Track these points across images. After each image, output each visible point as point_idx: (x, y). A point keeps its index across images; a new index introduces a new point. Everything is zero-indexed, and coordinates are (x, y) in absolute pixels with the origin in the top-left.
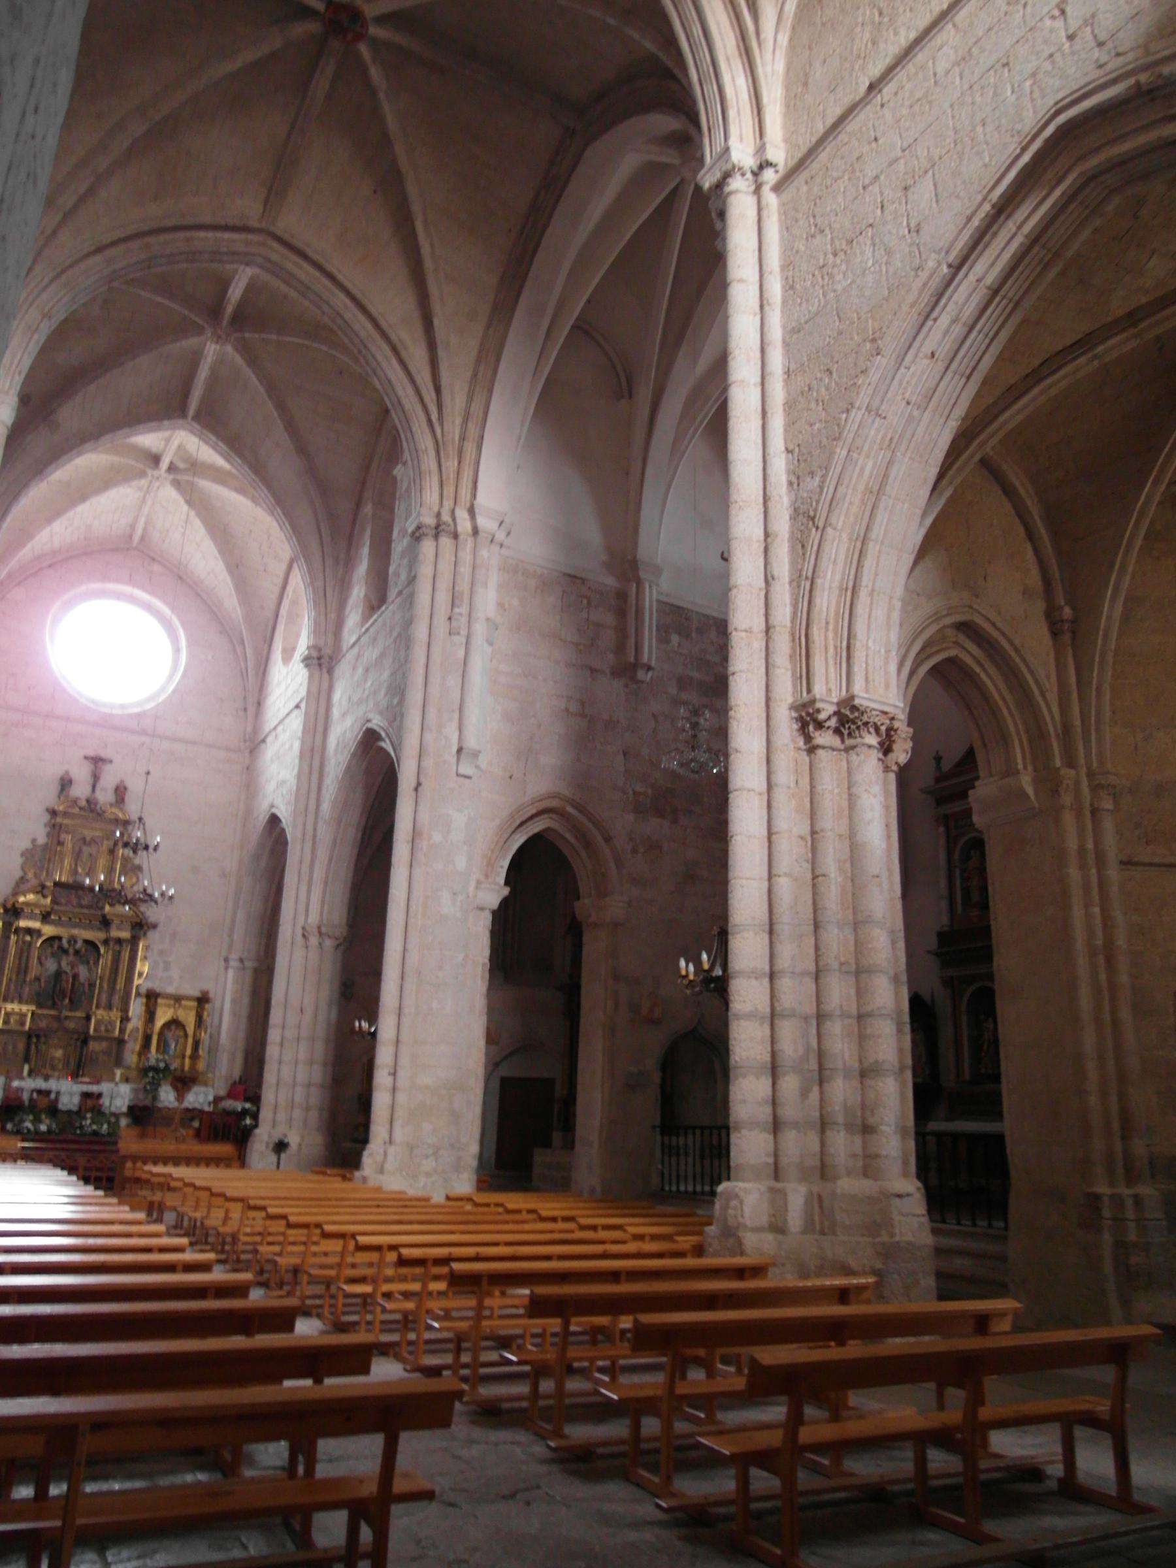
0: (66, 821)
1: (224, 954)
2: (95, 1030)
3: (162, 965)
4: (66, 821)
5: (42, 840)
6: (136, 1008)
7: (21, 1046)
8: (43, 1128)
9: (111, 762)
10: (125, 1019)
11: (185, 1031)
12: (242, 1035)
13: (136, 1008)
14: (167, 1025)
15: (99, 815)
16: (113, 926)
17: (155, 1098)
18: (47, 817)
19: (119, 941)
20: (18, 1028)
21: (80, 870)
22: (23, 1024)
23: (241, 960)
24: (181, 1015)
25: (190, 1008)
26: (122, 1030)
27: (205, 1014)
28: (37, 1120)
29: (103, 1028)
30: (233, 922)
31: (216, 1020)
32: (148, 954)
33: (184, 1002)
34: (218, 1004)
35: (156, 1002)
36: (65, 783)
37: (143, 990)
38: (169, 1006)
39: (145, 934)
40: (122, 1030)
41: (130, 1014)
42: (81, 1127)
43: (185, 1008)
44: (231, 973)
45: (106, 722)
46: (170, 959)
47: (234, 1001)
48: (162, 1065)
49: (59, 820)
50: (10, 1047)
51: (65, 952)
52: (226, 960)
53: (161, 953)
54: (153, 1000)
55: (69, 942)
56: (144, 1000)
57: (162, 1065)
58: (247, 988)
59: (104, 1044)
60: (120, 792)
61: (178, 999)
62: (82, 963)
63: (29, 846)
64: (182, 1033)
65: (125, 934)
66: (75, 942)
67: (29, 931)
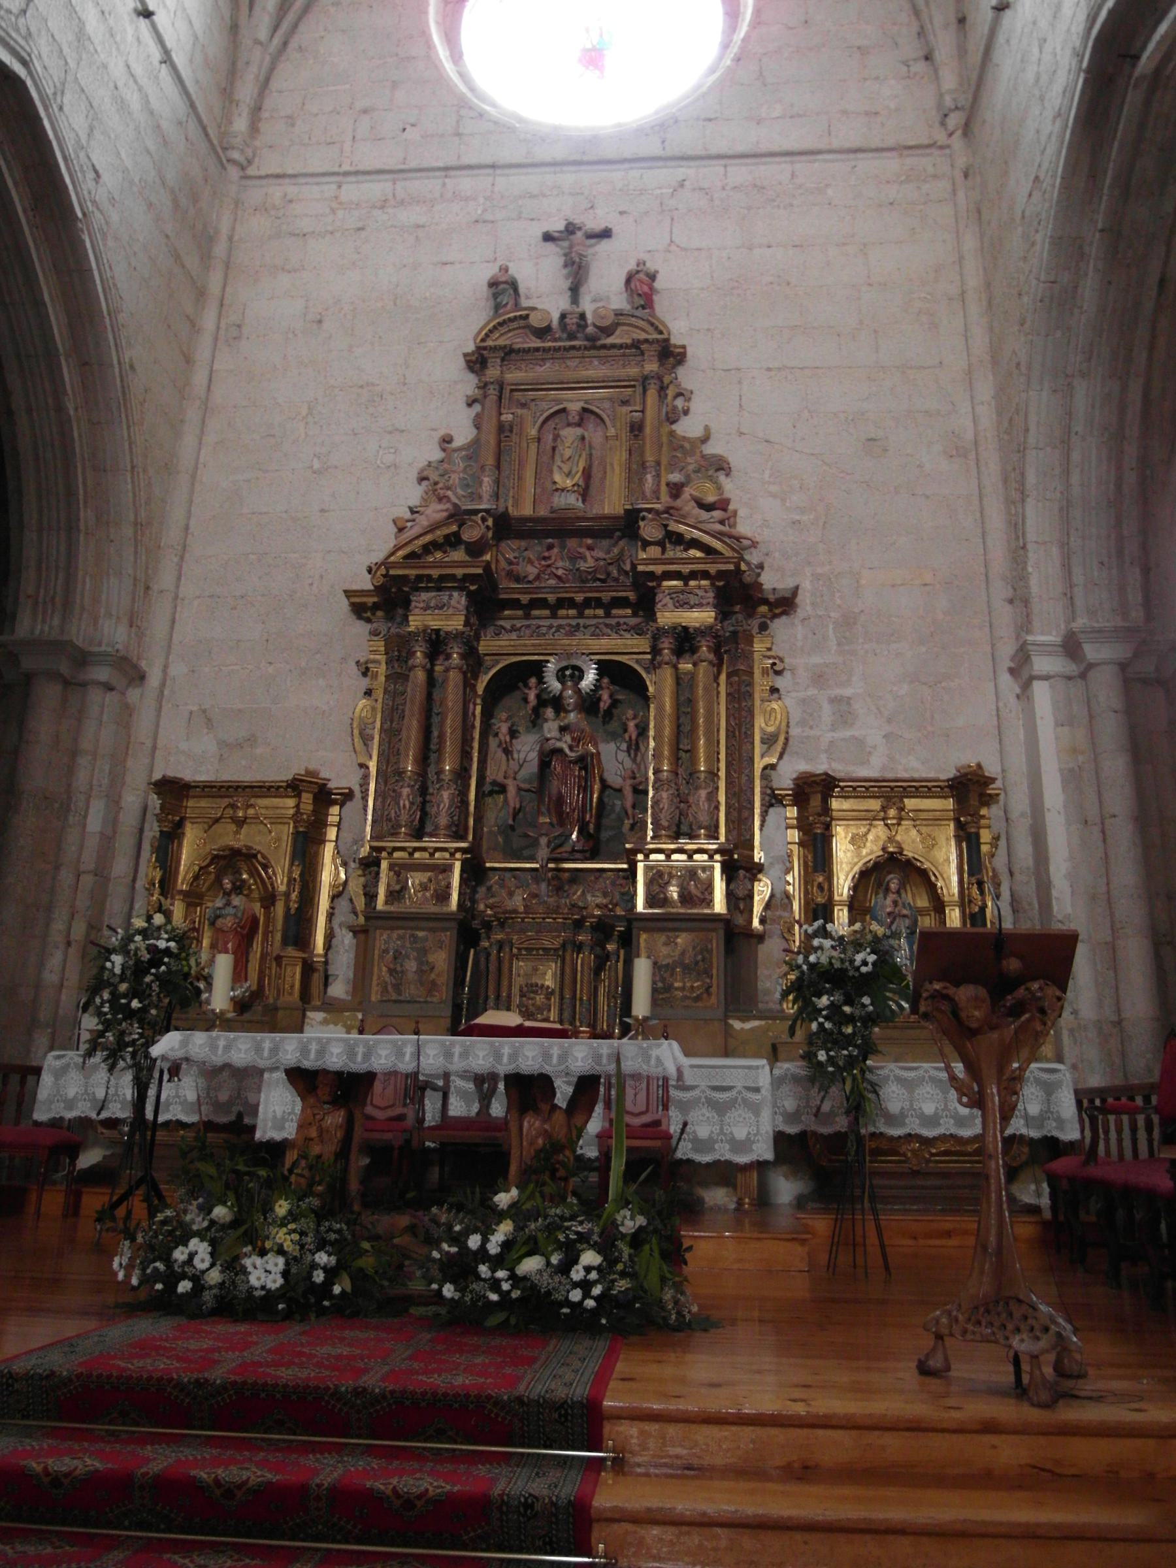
0: (513, 376)
1: (1007, 649)
2: (650, 901)
3: (827, 710)
4: (513, 376)
5: (463, 434)
6: (775, 837)
7: (441, 959)
8: (264, 1273)
9: (606, 234)
10: (741, 869)
11: (932, 888)
12: (1127, 875)
13: (775, 837)
14: (870, 877)
15: (592, 339)
16: (663, 599)
17: (857, 1106)
18: (469, 384)
19: (685, 640)
20: (432, 908)
21: (557, 477)
22: (444, 896)
23: (1071, 647)
24: (910, 841)
25: (936, 820)
26: (739, 900)
27: (985, 836)
28: (246, 1233)
29: (674, 892)
30: (1018, 553)
31: (1024, 850)
32: (780, 682)
33: (910, 803)
34: (1018, 801)
35: (826, 810)
36: (503, 288)
37: (785, 779)
38: (870, 818)
39: (763, 627)
40: (739, 900)
41: (758, 856)
42: (461, 1268)
43: (918, 818)
44: (1041, 691)
45: (587, 156)
46: (848, 692)
47: (1071, 778)
48: (865, 959)
49: (493, 372)
50: (411, 966)
51: (557, 703)
52: (1021, 666)
53: (819, 678)
54: (815, 802)
55: (560, 676)
56: (792, 812)
57: (865, 959)
58: (1111, 728)
59: (682, 939)
60: (642, 286)
61: (892, 794)
62: (614, 736)
63: (437, 455)
64: (923, 902)
65: (701, 617)
66: (579, 673)
67: (436, 643)
